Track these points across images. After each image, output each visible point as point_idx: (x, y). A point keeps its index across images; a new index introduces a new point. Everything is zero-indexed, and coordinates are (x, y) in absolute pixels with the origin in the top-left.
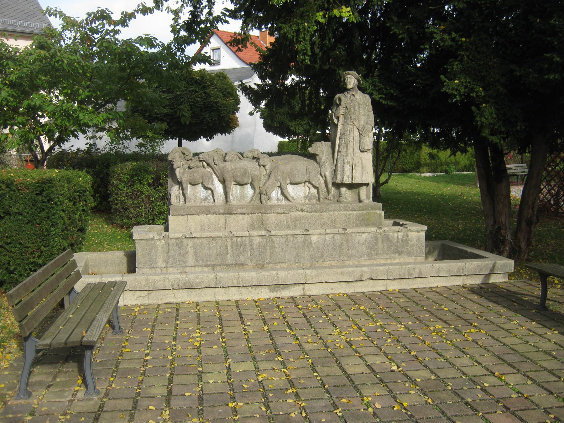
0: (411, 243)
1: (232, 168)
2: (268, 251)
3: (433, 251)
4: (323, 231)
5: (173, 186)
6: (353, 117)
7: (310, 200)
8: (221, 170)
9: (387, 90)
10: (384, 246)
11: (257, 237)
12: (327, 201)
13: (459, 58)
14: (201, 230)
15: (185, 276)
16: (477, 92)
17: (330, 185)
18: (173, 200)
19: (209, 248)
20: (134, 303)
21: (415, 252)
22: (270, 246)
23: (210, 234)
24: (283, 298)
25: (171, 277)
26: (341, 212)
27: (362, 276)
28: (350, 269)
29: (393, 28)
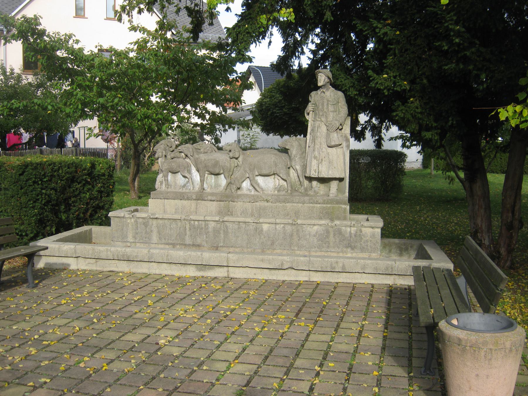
0: (365, 239)
1: (205, 160)
2: (222, 235)
4: (273, 220)
7: (278, 191)
10: (335, 239)
11: (212, 222)
13: (392, 52)
14: (176, 213)
15: (124, 249)
18: (157, 185)
19: (171, 229)
22: (224, 231)
24: (207, 278)
25: (113, 249)
26: (305, 205)
27: (282, 264)
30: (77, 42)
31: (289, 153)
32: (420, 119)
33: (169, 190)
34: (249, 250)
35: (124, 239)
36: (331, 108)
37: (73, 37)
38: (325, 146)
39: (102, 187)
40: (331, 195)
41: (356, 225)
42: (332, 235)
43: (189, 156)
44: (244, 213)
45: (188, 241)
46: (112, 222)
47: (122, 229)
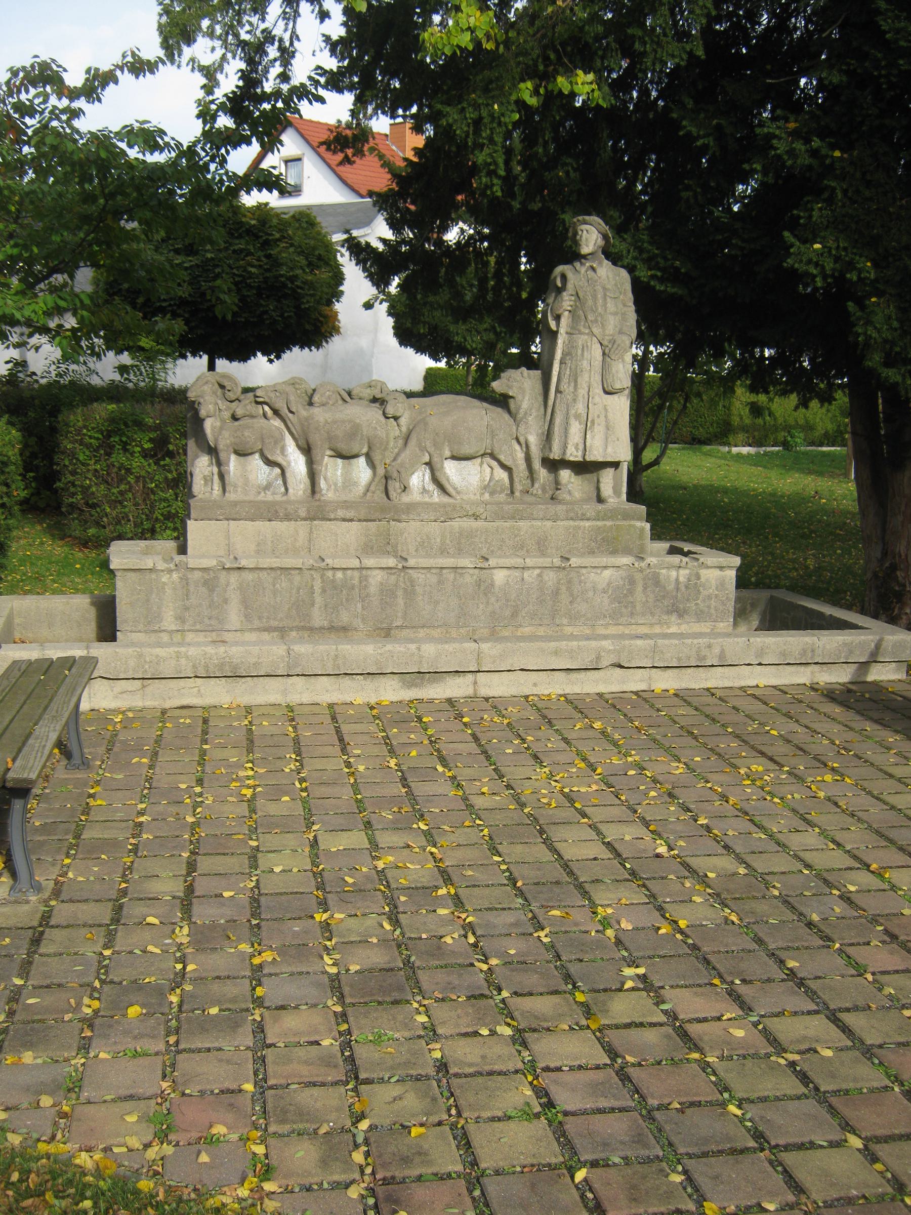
2: (401, 601)
4: (518, 562)
5: (197, 457)
6: (591, 317)
7: (492, 494)
8: (302, 425)
9: (665, 259)
10: (647, 596)
11: (377, 571)
12: (528, 498)
13: (826, 195)
14: (258, 552)
15: (222, 649)
16: (860, 271)
17: (537, 464)
18: (198, 486)
20: (113, 705)
21: (712, 611)
22: (405, 590)
23: (275, 562)
24: (431, 701)
25: (193, 651)
26: (559, 523)
27: (598, 658)
28: (575, 643)
29: (684, 123)
34: (463, 631)
42: (639, 588)
43: (284, 411)
44: (424, 546)
45: (318, 619)
47: (148, 600)
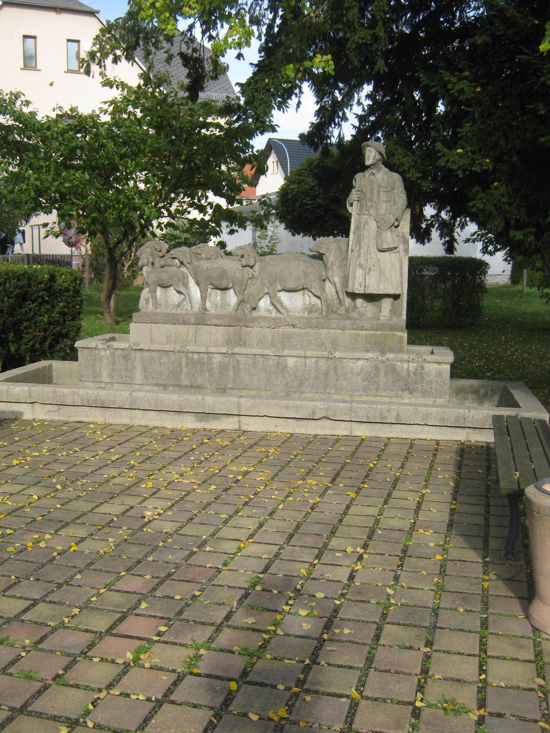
1: (207, 268)
2: (231, 373)
3: (492, 395)
4: (301, 353)
6: (369, 204)
7: (309, 312)
10: (387, 379)
11: (218, 355)
14: (167, 342)
15: (96, 392)
18: (142, 304)
21: (434, 391)
22: (234, 367)
24: (210, 431)
25: (81, 391)
26: (347, 331)
27: (314, 412)
30: (28, 103)
31: (325, 259)
32: (508, 212)
33: (158, 311)
34: (269, 393)
35: (96, 378)
36: (383, 197)
37: (22, 96)
38: (374, 250)
39: (65, 307)
40: (382, 318)
41: (416, 359)
42: (382, 373)
43: (185, 263)
44: (261, 343)
45: (184, 381)
46: (80, 355)
47: (94, 365)
